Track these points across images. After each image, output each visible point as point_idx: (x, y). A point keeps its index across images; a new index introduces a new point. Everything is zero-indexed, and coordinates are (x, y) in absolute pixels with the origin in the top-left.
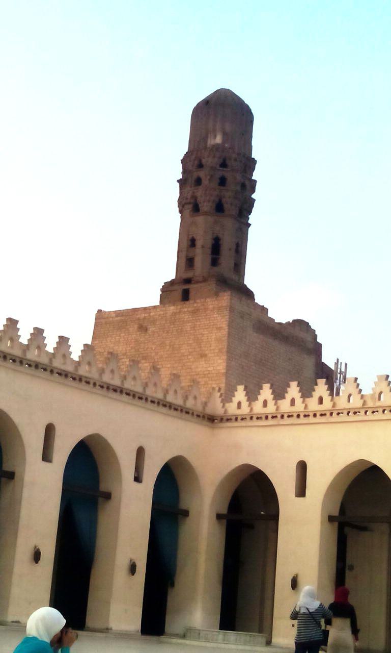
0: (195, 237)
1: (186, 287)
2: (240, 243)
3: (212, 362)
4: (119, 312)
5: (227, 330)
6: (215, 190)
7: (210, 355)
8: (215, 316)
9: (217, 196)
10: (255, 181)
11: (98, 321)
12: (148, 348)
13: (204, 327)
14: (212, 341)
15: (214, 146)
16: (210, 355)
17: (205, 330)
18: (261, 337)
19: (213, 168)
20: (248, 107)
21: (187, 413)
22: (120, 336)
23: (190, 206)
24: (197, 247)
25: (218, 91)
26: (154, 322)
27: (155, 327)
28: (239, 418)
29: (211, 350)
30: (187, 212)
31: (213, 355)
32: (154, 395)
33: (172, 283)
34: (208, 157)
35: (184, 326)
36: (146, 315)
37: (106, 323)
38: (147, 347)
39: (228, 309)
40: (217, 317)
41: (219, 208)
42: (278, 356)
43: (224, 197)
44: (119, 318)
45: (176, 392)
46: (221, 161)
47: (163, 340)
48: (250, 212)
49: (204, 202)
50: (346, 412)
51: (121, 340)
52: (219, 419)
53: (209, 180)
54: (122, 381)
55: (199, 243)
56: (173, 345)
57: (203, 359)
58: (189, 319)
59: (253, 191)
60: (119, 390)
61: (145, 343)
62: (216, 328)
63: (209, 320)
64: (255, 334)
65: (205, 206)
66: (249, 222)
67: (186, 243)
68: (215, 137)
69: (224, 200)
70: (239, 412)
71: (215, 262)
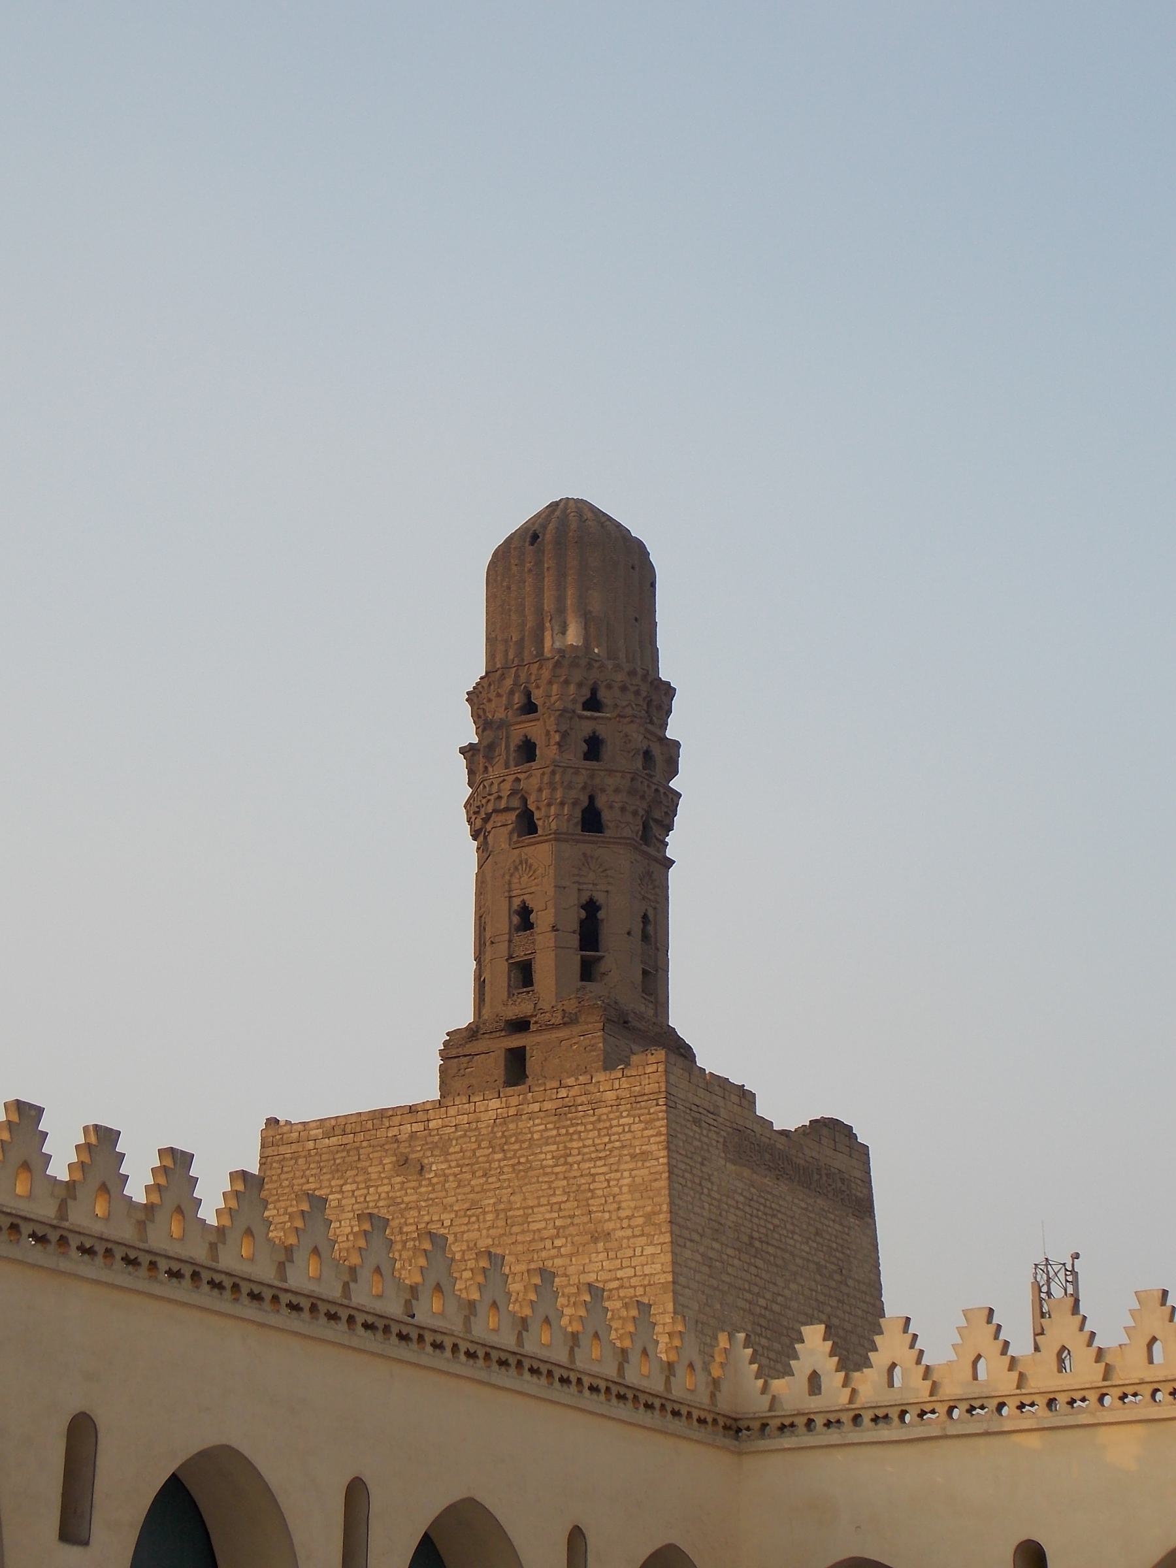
0: (531, 904)
1: (515, 1041)
2: (651, 917)
3: (630, 1253)
4: (333, 1122)
5: (664, 1160)
6: (577, 771)
7: (620, 1233)
8: (622, 1121)
9: (584, 788)
10: (677, 744)
11: (269, 1151)
12: (432, 1221)
13: (593, 1156)
14: (621, 1193)
15: (561, 652)
16: (620, 1233)
17: (599, 1163)
18: (746, 1172)
19: (565, 713)
20: (640, 546)
21: (676, 1414)
22: (341, 1192)
23: (512, 817)
24: (537, 929)
25: (554, 506)
26: (442, 1147)
27: (447, 1161)
28: (820, 1421)
29: (619, 1218)
30: (500, 837)
31: (629, 1232)
32: (595, 1369)
33: (472, 1033)
34: (550, 683)
35: (533, 1154)
36: (415, 1127)
37: (295, 1157)
38: (427, 1218)
39: (661, 1101)
40: (630, 1125)
41: (591, 820)
42: (789, 1227)
43: (603, 790)
44: (334, 1140)
45: (645, 1352)
46: (586, 693)
47: (471, 1196)
48: (669, 828)
49: (549, 805)
50: (1147, 1390)
51: (344, 1202)
52: (756, 1425)
53: (558, 744)
54: (520, 1334)
55: (543, 919)
56: (505, 1210)
57: (601, 1245)
58: (546, 1134)
59: (674, 772)
60: (512, 1361)
61: (419, 1209)
62: (633, 1156)
63: (608, 1135)
64: (728, 1165)
65: (549, 819)
66: (669, 853)
67: (502, 923)
68: (564, 633)
69: (601, 802)
70: (814, 1404)
71: (588, 971)
